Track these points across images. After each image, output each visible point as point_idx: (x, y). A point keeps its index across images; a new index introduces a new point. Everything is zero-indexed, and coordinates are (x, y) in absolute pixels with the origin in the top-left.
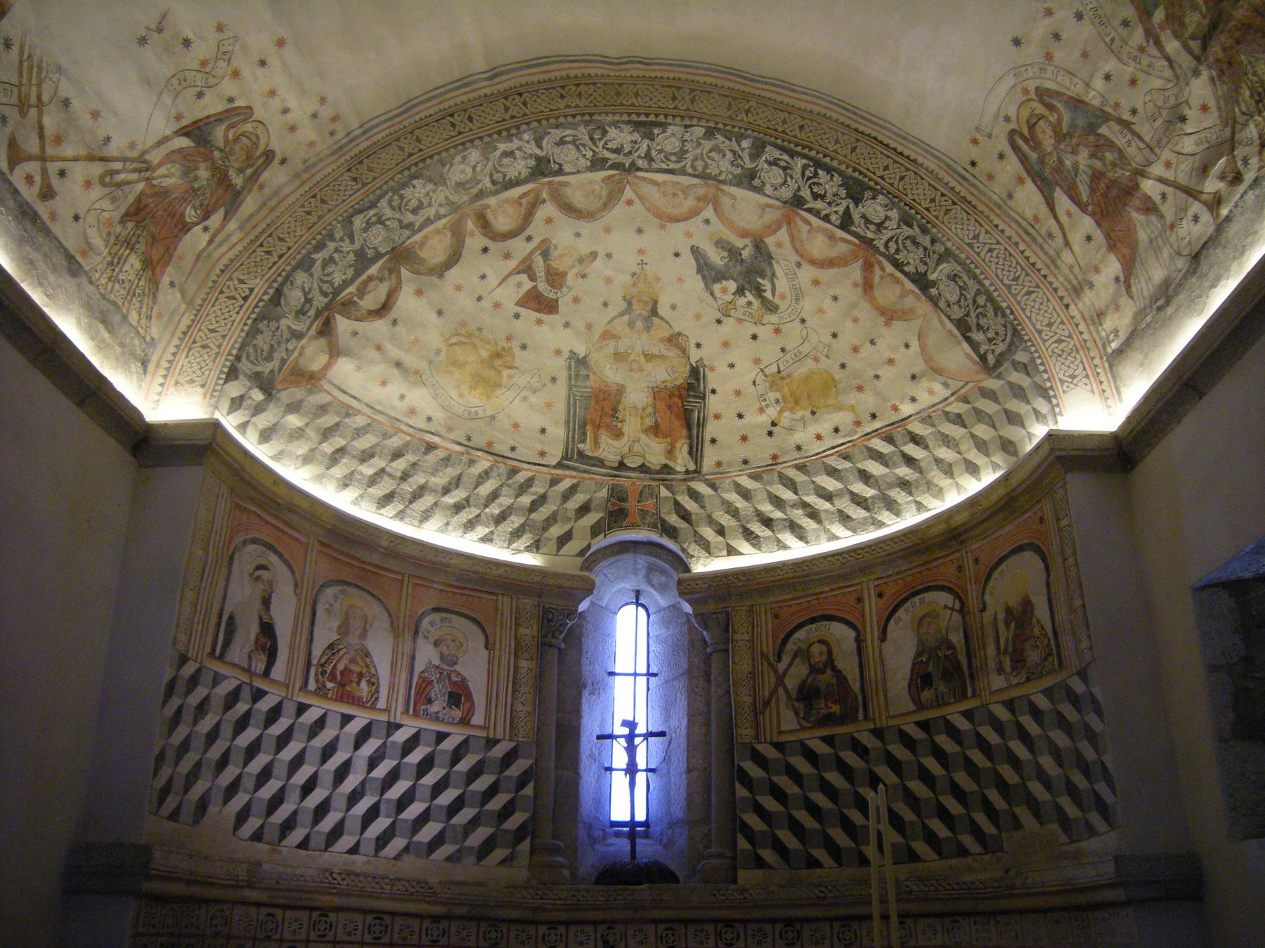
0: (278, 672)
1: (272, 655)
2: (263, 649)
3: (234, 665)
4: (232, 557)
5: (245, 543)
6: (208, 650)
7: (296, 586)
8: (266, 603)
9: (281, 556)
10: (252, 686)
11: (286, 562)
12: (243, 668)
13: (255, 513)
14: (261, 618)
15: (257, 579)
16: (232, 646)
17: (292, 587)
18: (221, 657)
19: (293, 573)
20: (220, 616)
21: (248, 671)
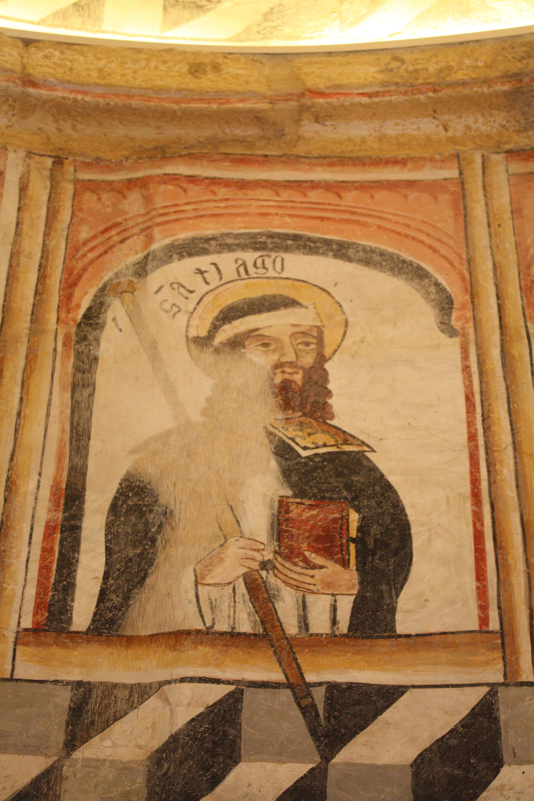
0: (437, 591)
1: (384, 550)
2: (329, 543)
3: (177, 638)
4: (93, 319)
5: (141, 270)
6: (22, 609)
7: (445, 305)
8: (304, 395)
9: (341, 251)
10: (300, 689)
11: (370, 258)
12: (233, 637)
13: (173, 179)
14: (283, 451)
15: (236, 343)
16: (157, 578)
17: (427, 316)
18: (108, 625)
19: (417, 274)
20: (71, 497)
21: (268, 635)
